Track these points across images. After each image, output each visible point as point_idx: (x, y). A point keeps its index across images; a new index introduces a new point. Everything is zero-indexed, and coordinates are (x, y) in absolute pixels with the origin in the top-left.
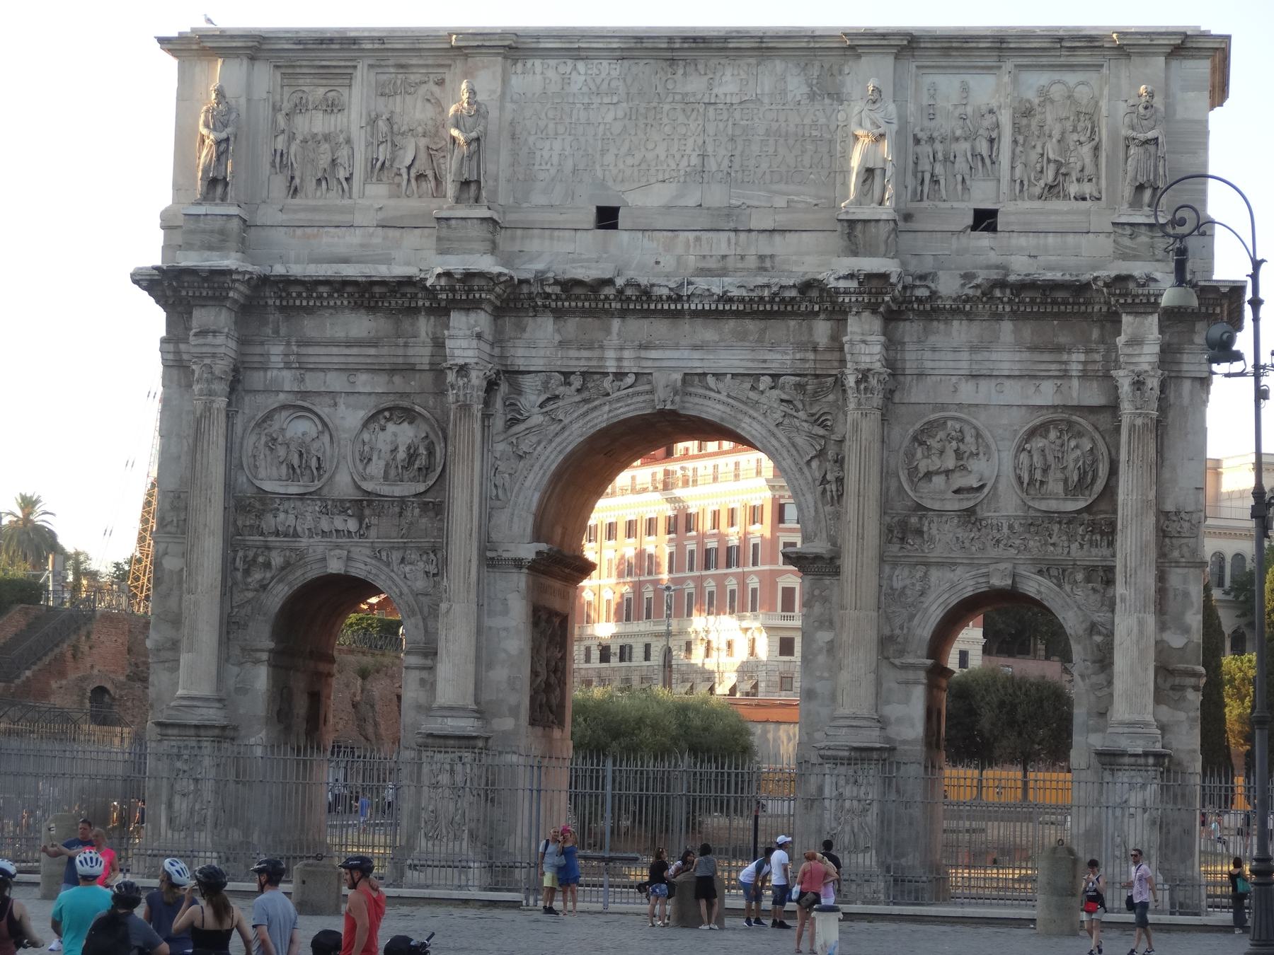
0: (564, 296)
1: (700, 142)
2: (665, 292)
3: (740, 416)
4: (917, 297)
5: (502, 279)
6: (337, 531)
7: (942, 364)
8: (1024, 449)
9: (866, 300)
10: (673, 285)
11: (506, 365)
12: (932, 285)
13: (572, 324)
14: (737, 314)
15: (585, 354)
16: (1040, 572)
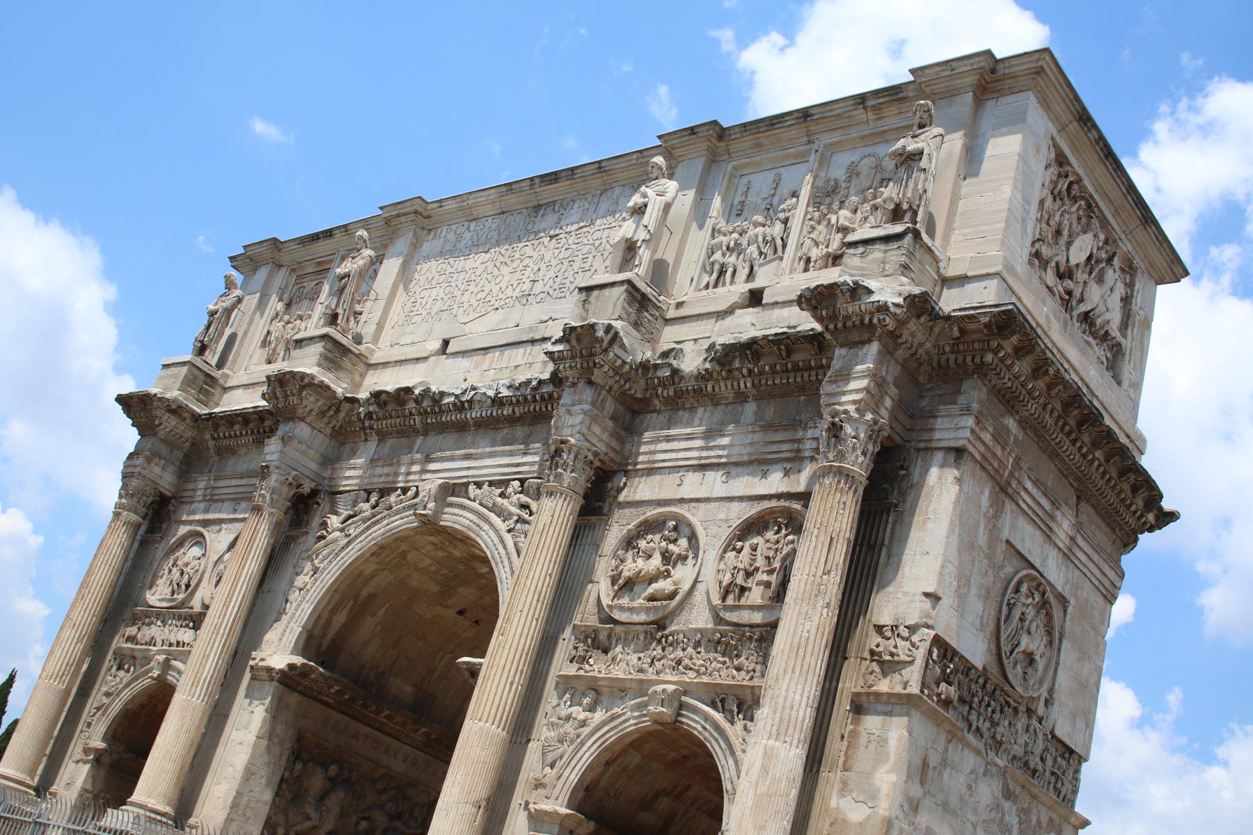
0: (381, 415)
1: (536, 269)
2: (452, 399)
3: (482, 524)
4: (659, 378)
5: (306, 381)
6: (178, 643)
7: (673, 456)
8: (734, 549)
9: (578, 366)
10: (458, 392)
11: (331, 486)
12: (675, 363)
13: (390, 443)
14: (512, 421)
15: (386, 470)
16: (713, 705)
